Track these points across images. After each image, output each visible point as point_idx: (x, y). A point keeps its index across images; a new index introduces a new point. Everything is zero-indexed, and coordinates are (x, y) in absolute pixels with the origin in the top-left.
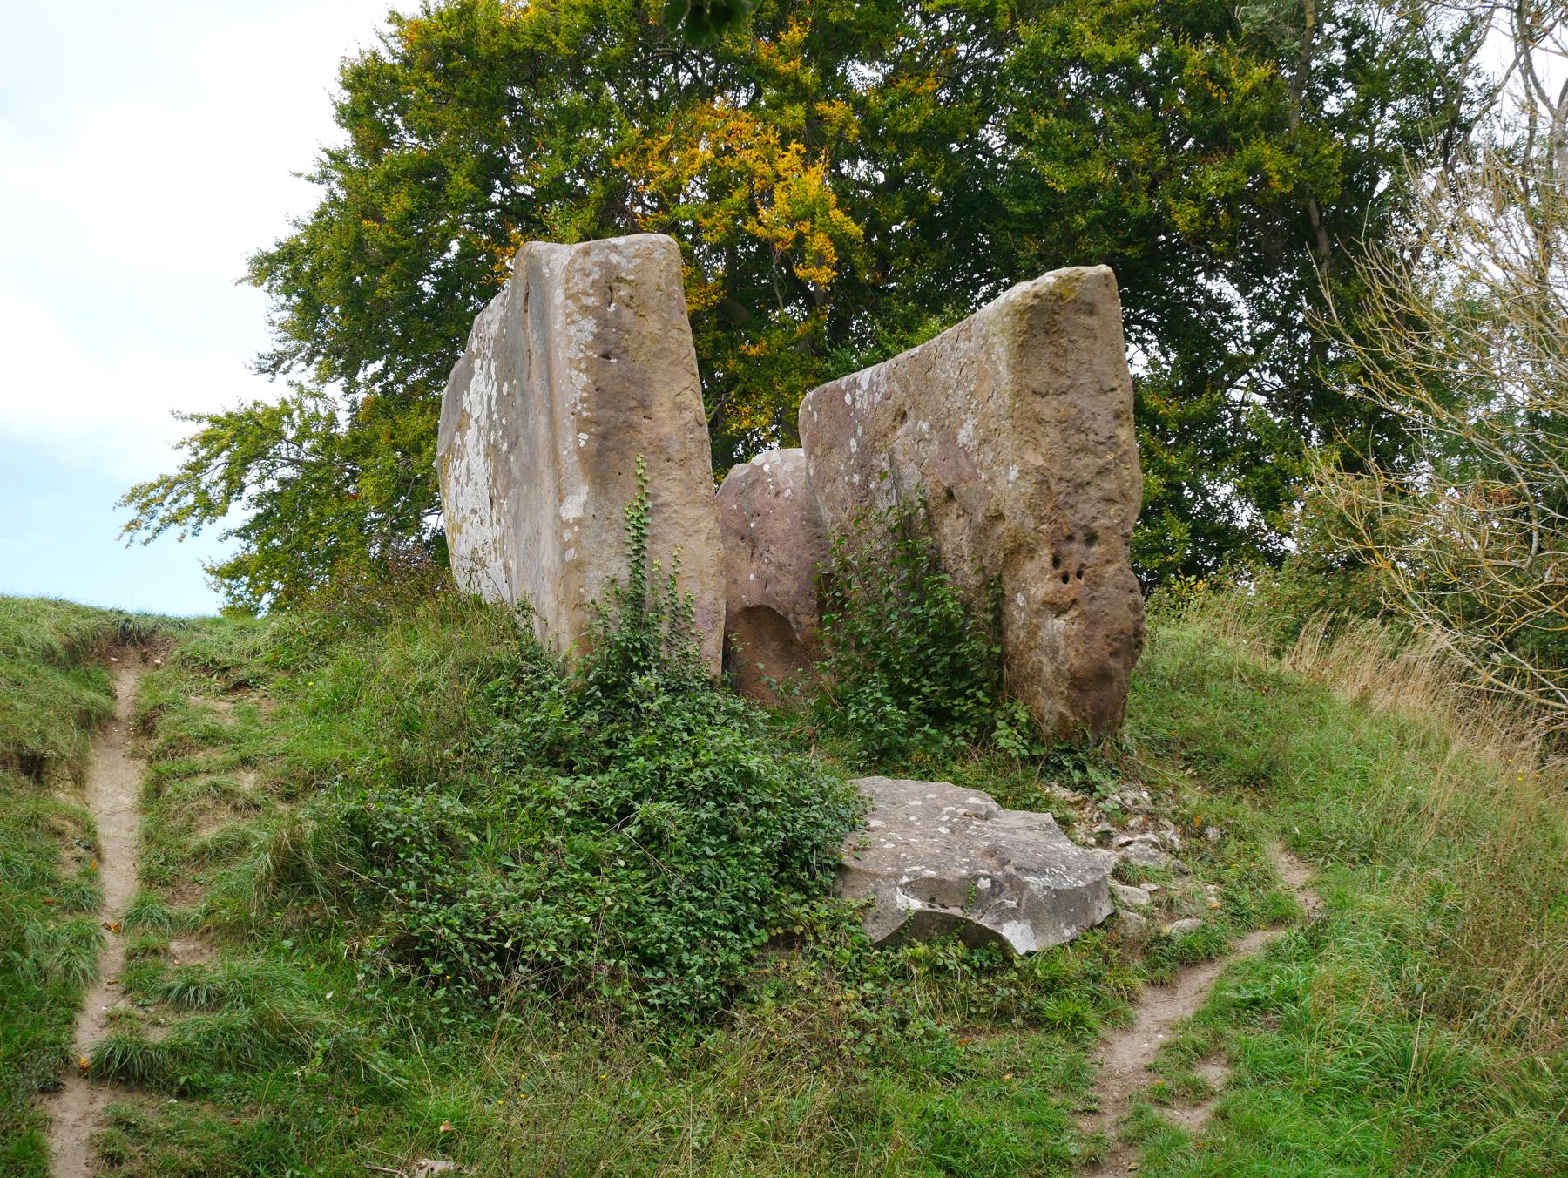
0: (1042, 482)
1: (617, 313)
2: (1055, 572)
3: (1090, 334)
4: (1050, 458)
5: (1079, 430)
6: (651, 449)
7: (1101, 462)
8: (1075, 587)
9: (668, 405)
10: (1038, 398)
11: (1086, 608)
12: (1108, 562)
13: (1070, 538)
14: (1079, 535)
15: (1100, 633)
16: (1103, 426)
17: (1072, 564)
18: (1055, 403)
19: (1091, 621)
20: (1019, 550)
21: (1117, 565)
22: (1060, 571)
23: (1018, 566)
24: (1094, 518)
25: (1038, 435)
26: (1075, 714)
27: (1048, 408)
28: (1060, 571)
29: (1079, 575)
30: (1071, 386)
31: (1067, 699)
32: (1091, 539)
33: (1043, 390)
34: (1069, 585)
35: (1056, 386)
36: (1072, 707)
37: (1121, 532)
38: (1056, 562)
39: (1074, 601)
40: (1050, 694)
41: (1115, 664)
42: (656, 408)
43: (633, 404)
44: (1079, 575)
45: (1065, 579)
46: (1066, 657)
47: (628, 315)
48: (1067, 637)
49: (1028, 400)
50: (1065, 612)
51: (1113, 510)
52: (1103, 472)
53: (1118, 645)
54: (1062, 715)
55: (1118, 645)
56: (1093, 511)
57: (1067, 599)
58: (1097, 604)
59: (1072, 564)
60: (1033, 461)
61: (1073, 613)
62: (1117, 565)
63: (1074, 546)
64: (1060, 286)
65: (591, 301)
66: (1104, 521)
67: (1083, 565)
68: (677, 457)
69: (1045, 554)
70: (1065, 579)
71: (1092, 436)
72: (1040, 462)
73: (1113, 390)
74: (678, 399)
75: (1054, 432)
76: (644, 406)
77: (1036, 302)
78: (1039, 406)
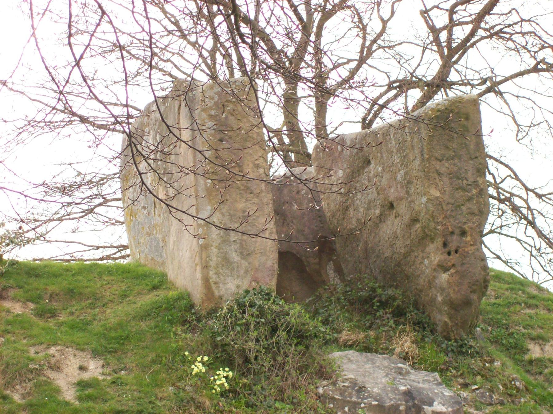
1: (226, 118)
2: (443, 250)
4: (443, 193)
5: (458, 178)
6: (242, 188)
8: (454, 258)
9: (251, 165)
10: (439, 162)
11: (459, 268)
12: (471, 245)
13: (452, 233)
14: (457, 231)
17: (452, 246)
18: (447, 165)
19: (462, 275)
20: (426, 238)
22: (447, 250)
23: (425, 246)
24: (465, 223)
25: (437, 181)
26: (452, 322)
28: (447, 250)
29: (456, 252)
31: (448, 314)
33: (440, 158)
34: (451, 257)
35: (447, 156)
36: (450, 318)
37: (478, 230)
38: (445, 245)
39: (453, 265)
40: (440, 311)
41: (474, 297)
42: (245, 167)
44: (456, 252)
45: (449, 254)
47: (231, 118)
49: (433, 163)
50: (448, 270)
51: (475, 218)
52: (470, 199)
53: (475, 287)
54: (446, 322)
55: (475, 287)
57: (449, 264)
59: (452, 246)
60: (434, 194)
61: (452, 271)
63: (455, 237)
64: (450, 106)
65: (213, 112)
66: (470, 224)
67: (459, 247)
69: (439, 241)
70: (449, 254)
71: (465, 182)
72: (438, 194)
73: (476, 158)
74: (257, 162)
75: (446, 179)
77: (439, 113)
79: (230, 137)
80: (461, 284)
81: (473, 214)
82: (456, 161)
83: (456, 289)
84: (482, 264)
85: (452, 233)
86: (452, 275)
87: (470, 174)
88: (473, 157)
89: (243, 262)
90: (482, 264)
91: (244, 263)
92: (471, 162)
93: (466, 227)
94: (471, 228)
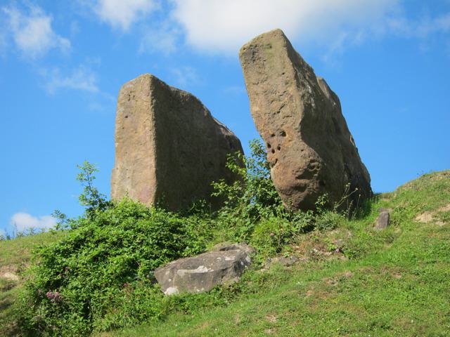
0: (259, 116)
3: (272, 55)
7: (282, 103)
11: (282, 161)
12: (290, 141)
13: (273, 135)
15: (290, 170)
16: (281, 89)
17: (274, 146)
18: (262, 86)
19: (286, 166)
21: (294, 141)
22: (271, 149)
27: (259, 89)
28: (271, 149)
29: (279, 149)
30: (267, 78)
32: (284, 134)
43: (132, 129)
58: (287, 158)
61: (277, 164)
62: (294, 141)
63: (275, 138)
68: (143, 143)
75: (262, 97)
76: (136, 130)
78: (255, 88)
79: (132, 113)
80: (285, 173)
82: (269, 80)
85: (273, 135)
87: (280, 87)
88: (281, 73)
89: (133, 190)
91: (134, 191)
92: (281, 78)
93: (284, 128)
94: (288, 128)
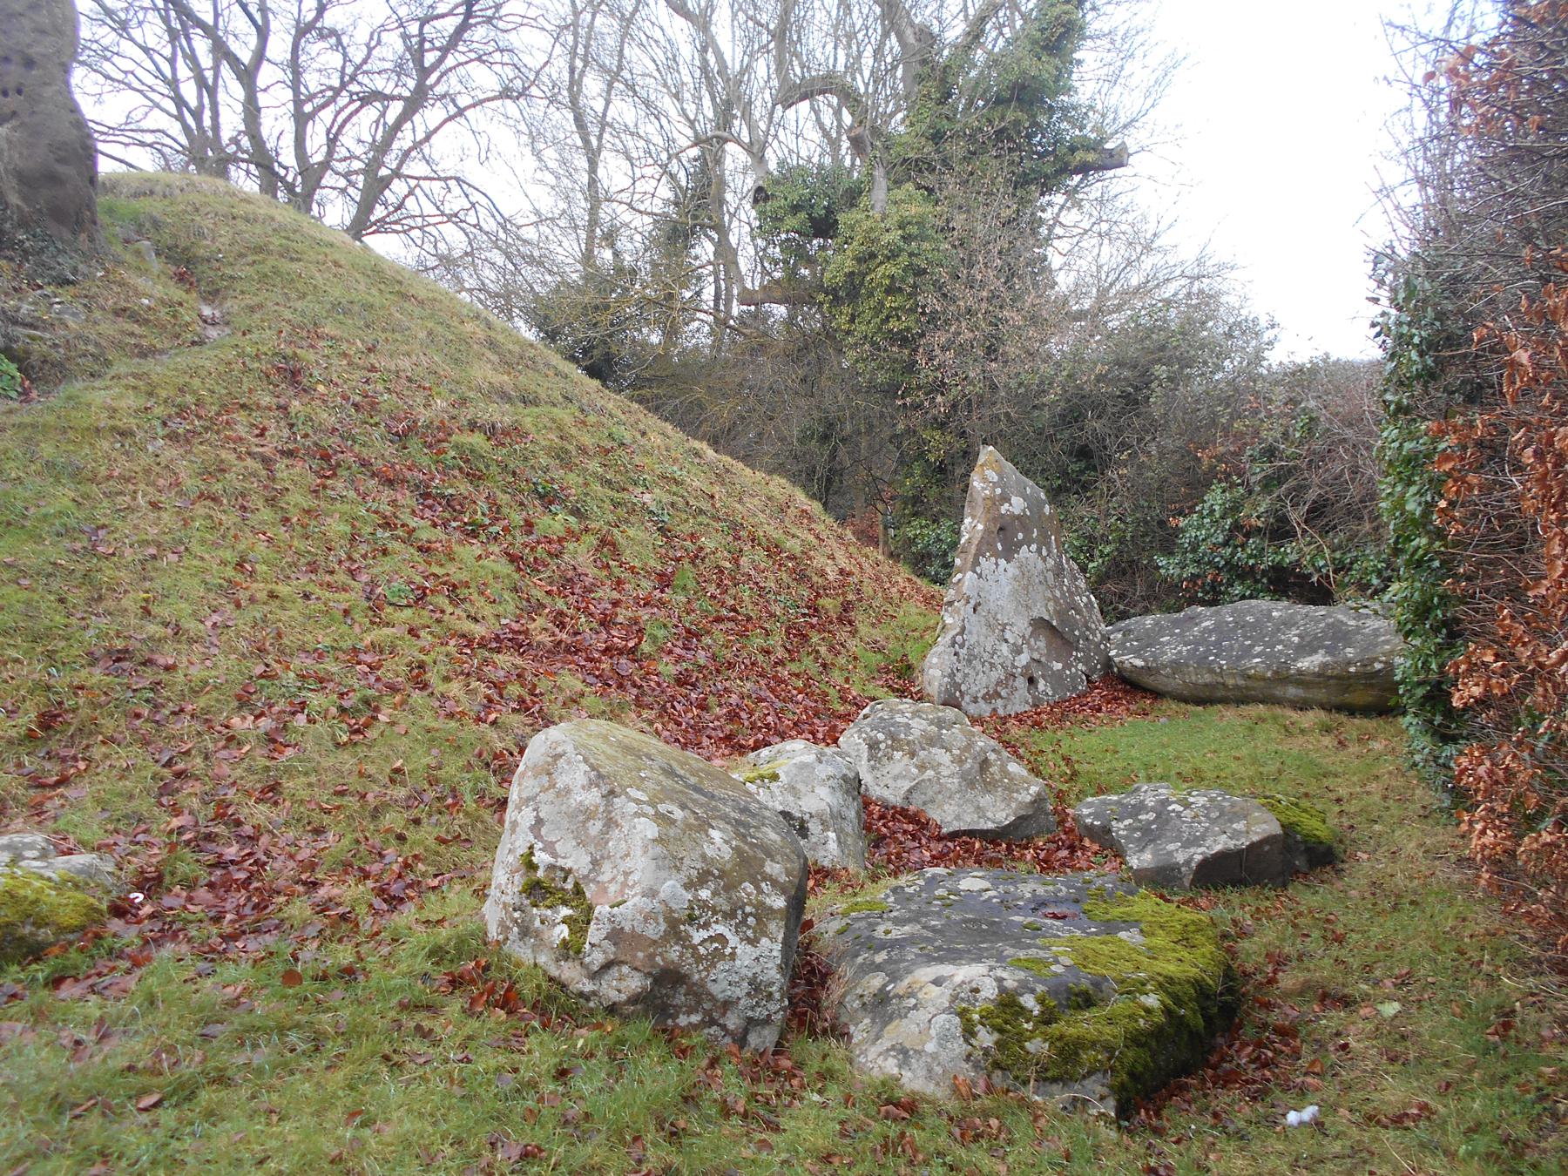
11: (27, 120)
12: (45, 84)
14: (16, 58)
24: (29, 46)
31: (20, 192)
36: (25, 199)
39: (14, 114)
44: (19, 92)
46: (11, 157)
48: (9, 141)
56: (28, 41)
61: (14, 122)
63: (12, 67)
81: (43, 32)
83: (25, 152)
84: (72, 117)
86: (14, 129)
90: (72, 117)
93: (33, 52)
